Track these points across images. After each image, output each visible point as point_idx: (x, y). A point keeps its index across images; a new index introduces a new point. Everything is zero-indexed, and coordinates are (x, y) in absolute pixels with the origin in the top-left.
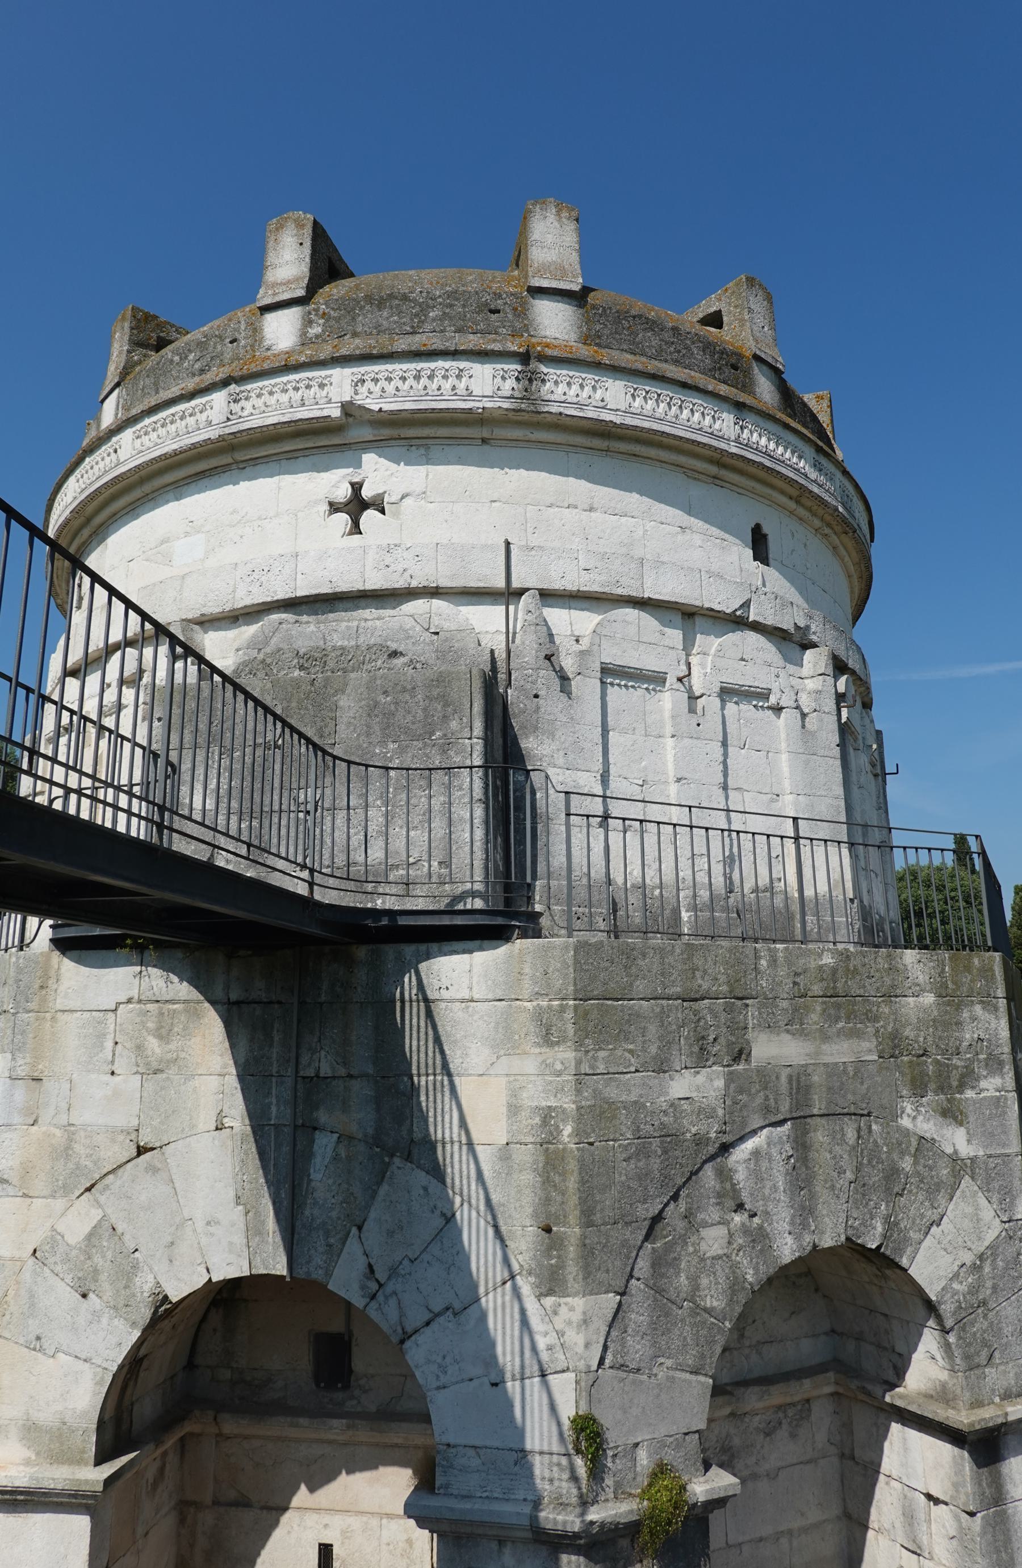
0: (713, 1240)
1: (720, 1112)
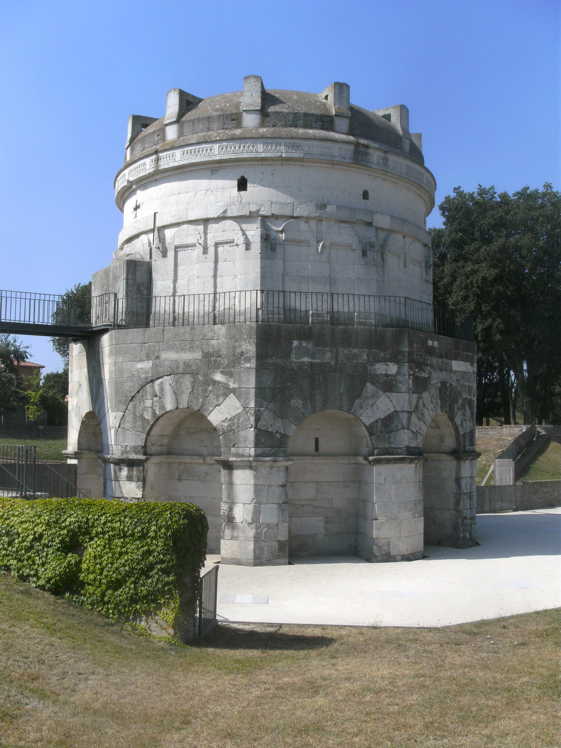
0: (148, 403)
1: (150, 372)
